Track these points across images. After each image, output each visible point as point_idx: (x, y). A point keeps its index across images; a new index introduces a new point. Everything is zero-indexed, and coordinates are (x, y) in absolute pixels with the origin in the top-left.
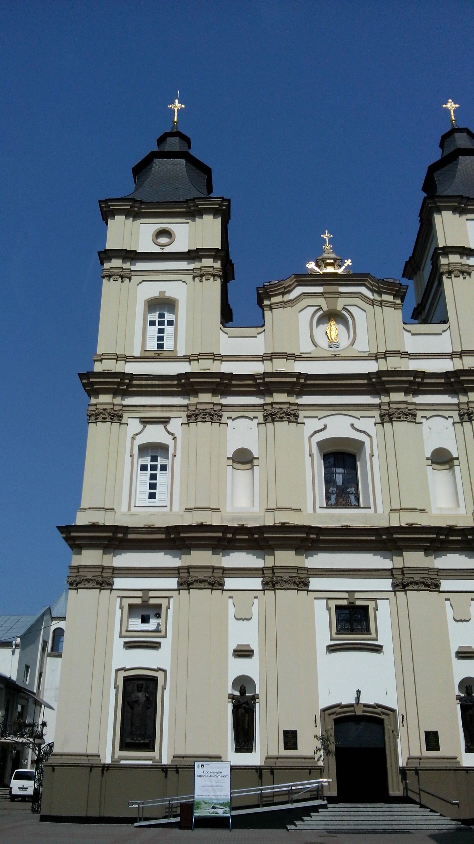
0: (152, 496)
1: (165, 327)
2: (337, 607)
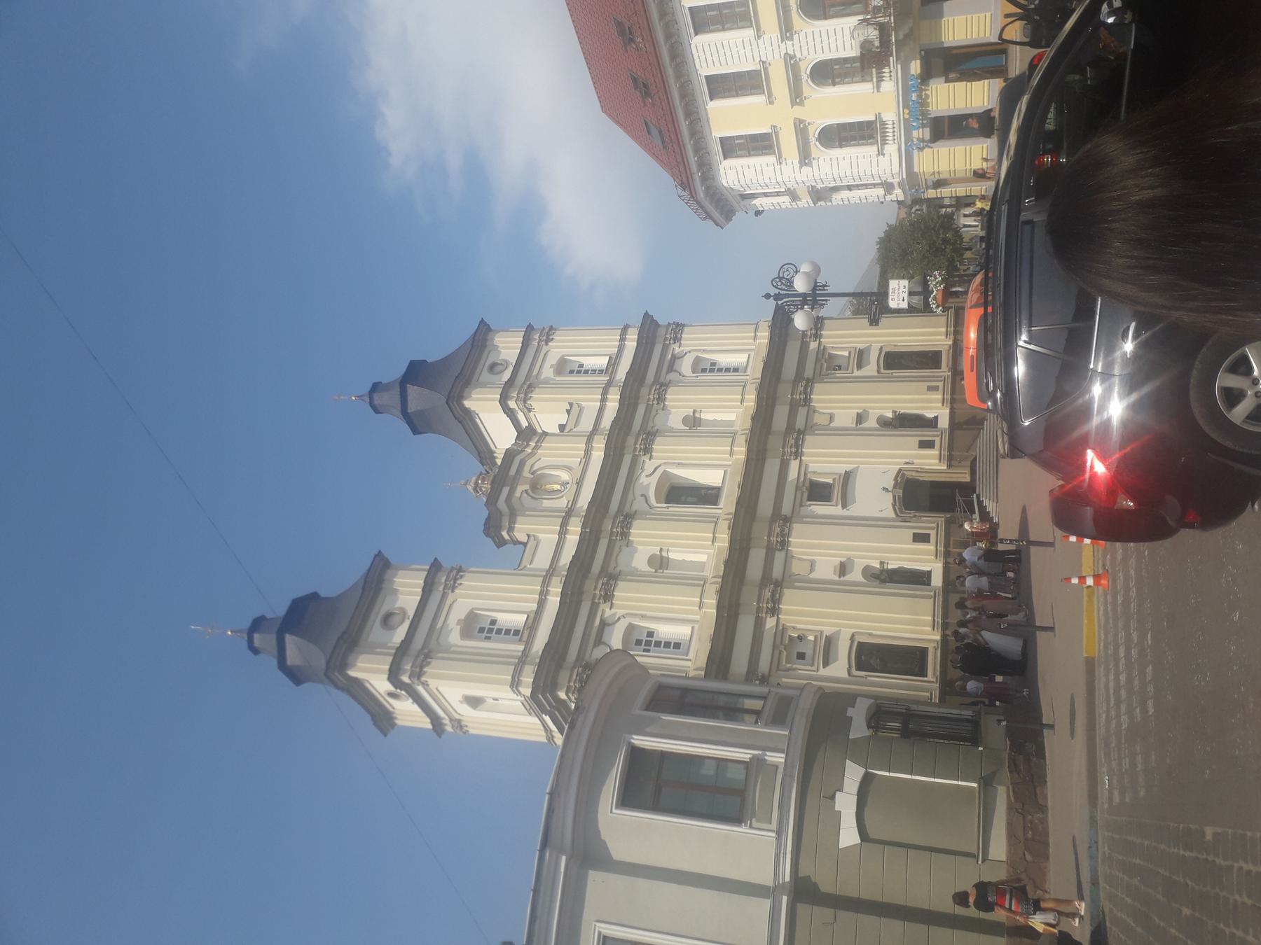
0: (677, 645)
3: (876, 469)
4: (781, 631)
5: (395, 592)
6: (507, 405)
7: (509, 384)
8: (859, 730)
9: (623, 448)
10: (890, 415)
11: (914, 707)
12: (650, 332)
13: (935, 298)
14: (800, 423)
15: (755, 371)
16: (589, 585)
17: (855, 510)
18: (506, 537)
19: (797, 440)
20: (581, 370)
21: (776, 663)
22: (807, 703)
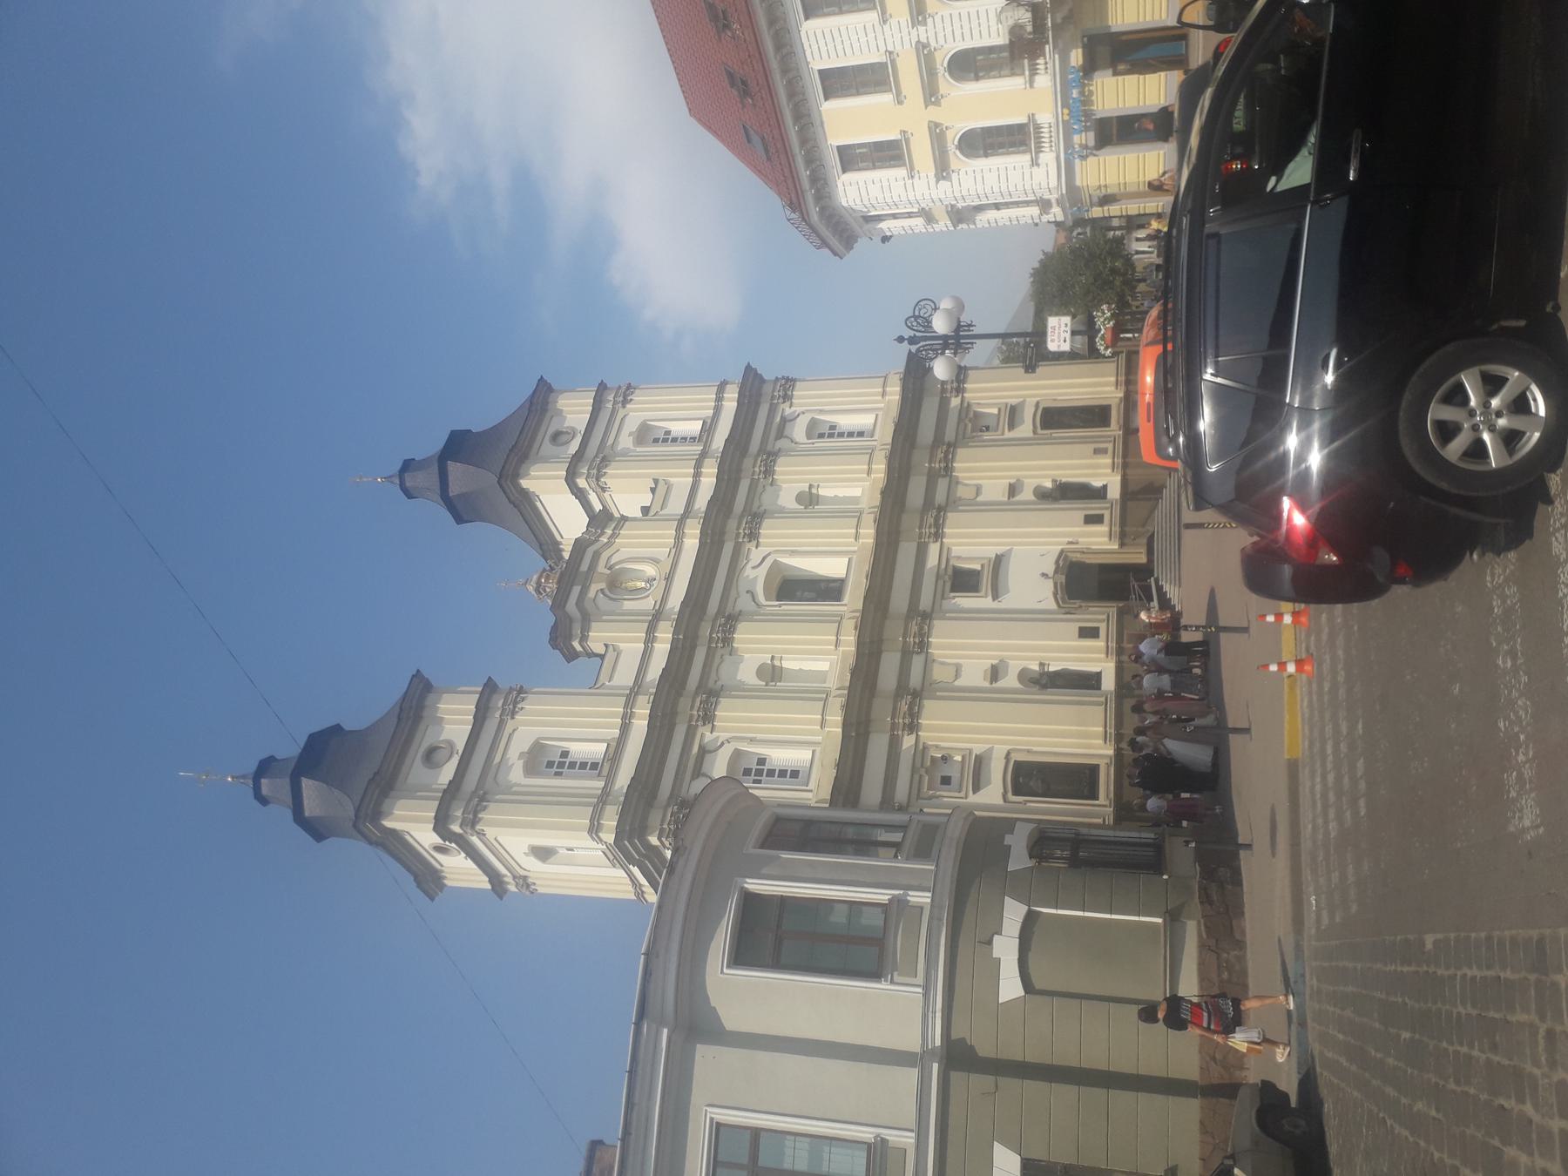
0: (795, 774)
1: (568, 760)
2: (953, 590)
3: (1033, 549)
4: (921, 751)
5: (439, 721)
6: (576, 485)
7: (578, 457)
8: (1019, 860)
9: (722, 533)
10: (1049, 484)
11: (1084, 831)
12: (753, 389)
13: (1103, 338)
14: (940, 497)
15: (885, 435)
16: (684, 703)
17: (1006, 602)
18: (578, 648)
19: (937, 519)
20: (668, 438)
21: (916, 791)
22: (956, 831)
